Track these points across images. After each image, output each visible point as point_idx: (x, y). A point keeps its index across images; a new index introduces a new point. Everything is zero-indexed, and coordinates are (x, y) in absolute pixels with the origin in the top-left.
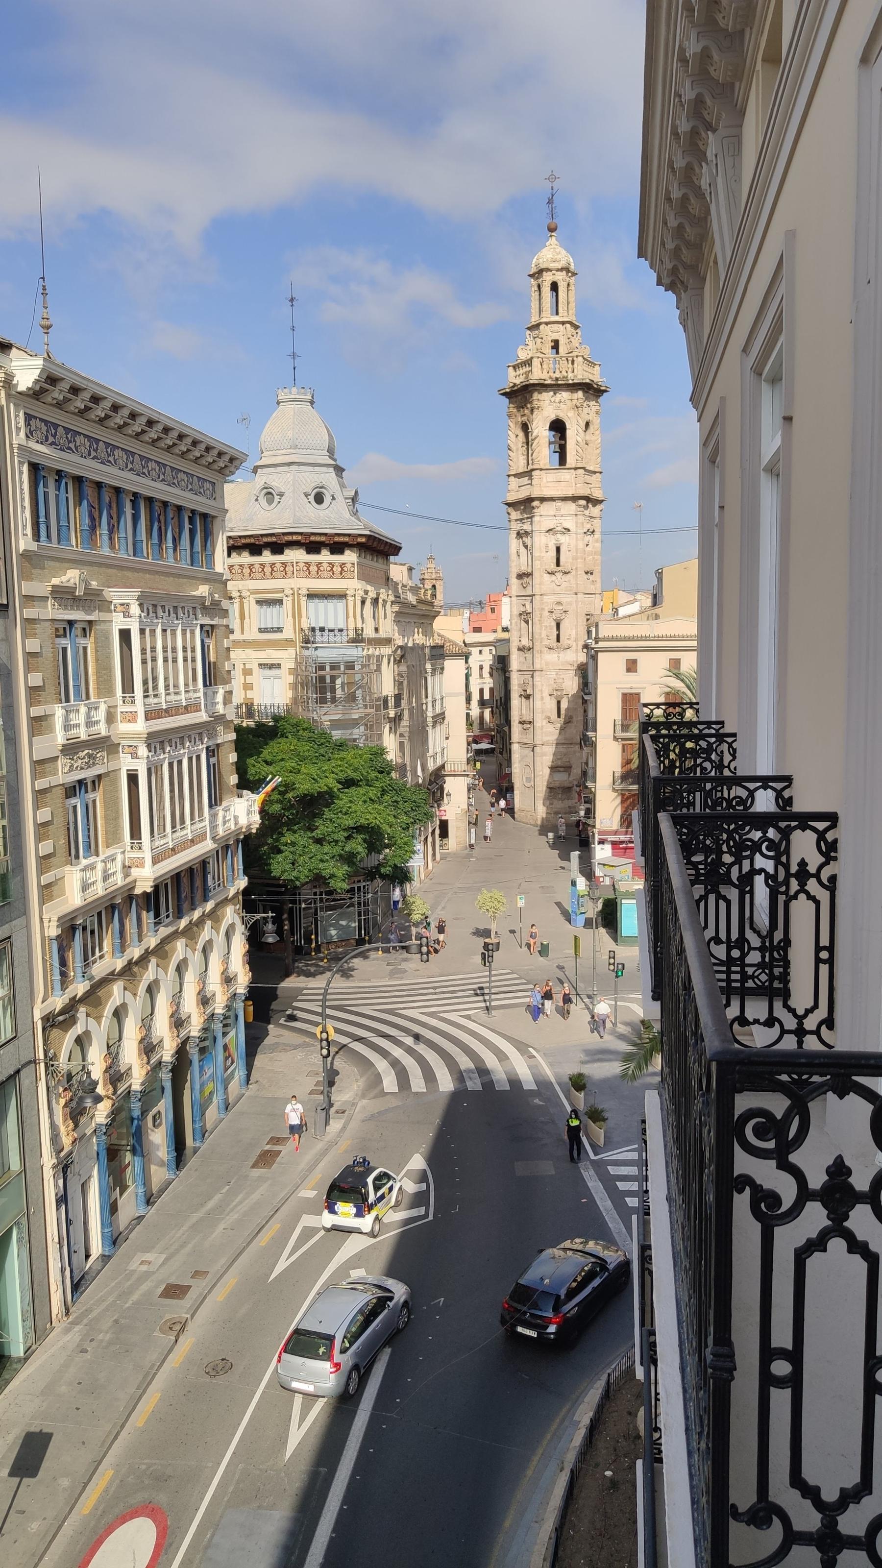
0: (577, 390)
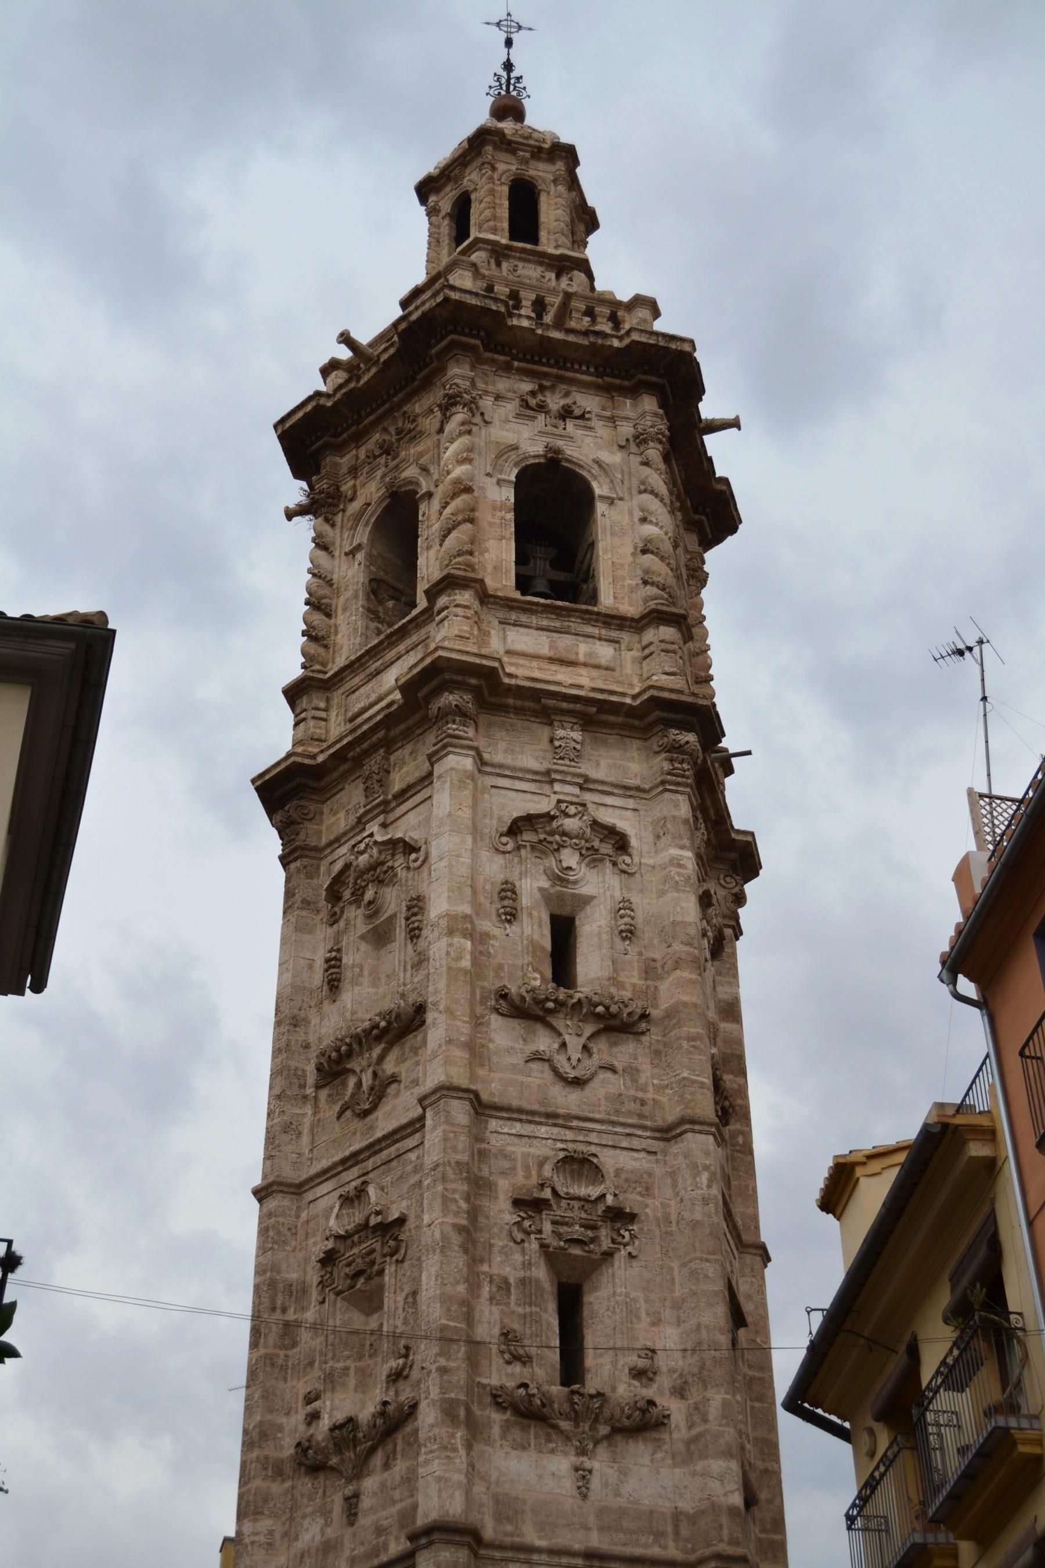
0: (633, 392)
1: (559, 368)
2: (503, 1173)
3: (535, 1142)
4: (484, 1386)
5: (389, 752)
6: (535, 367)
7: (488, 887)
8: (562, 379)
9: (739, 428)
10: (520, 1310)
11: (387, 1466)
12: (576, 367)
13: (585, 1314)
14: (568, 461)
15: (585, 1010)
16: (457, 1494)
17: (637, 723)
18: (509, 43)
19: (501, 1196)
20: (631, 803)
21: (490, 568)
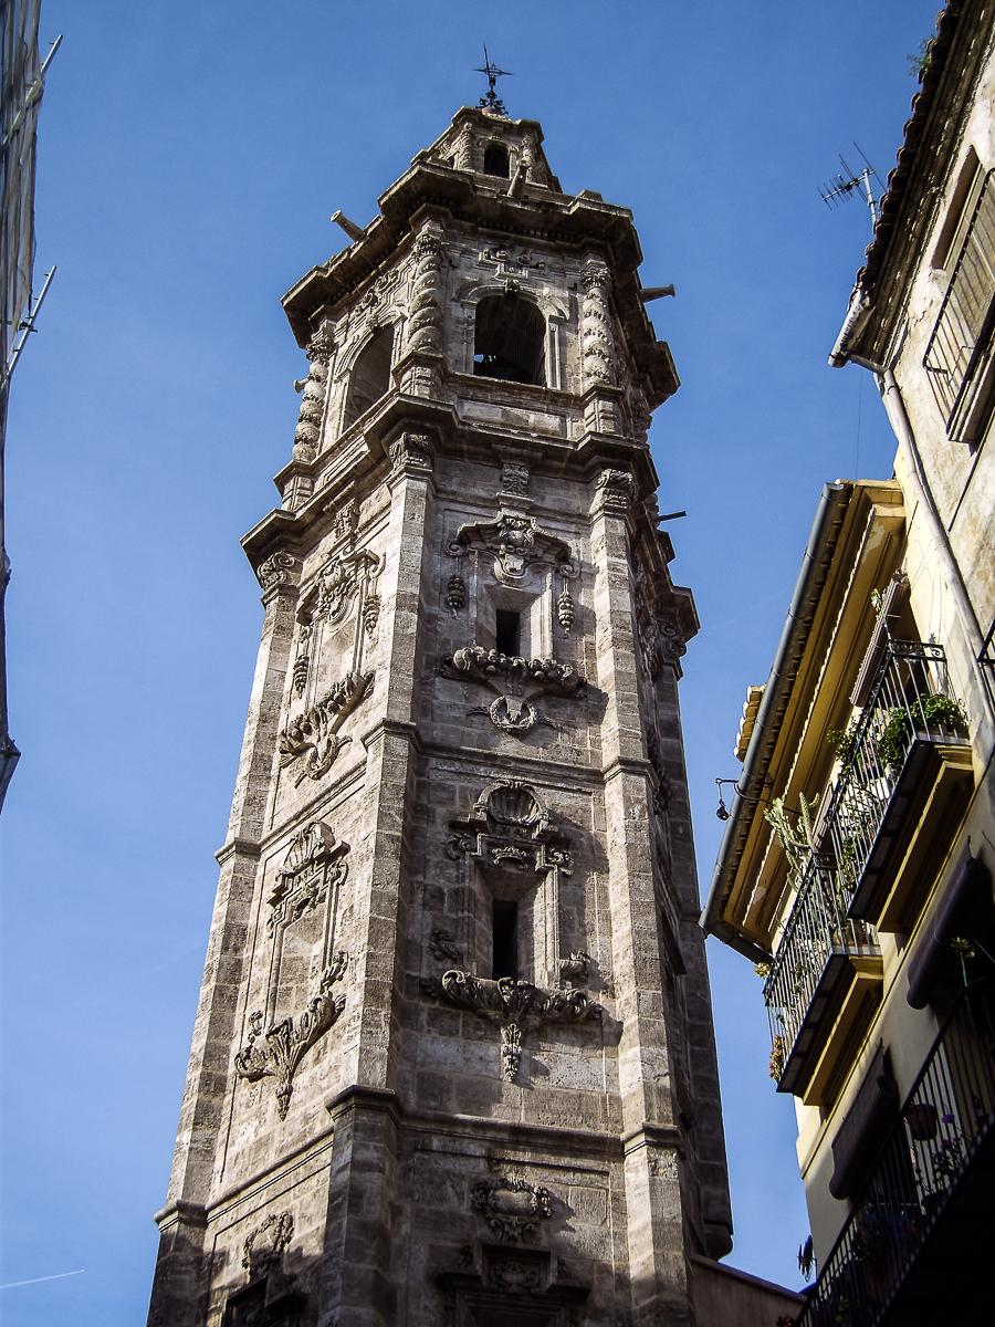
0: (580, 253)
1: (518, 233)
2: (442, 803)
3: (474, 779)
4: (413, 978)
5: (359, 502)
7: (438, 581)
8: (521, 243)
9: (673, 294)
10: (453, 916)
12: (532, 232)
14: (523, 295)
15: (525, 674)
16: (378, 1065)
17: (579, 468)
18: (493, 81)
19: (438, 821)
20: (573, 528)
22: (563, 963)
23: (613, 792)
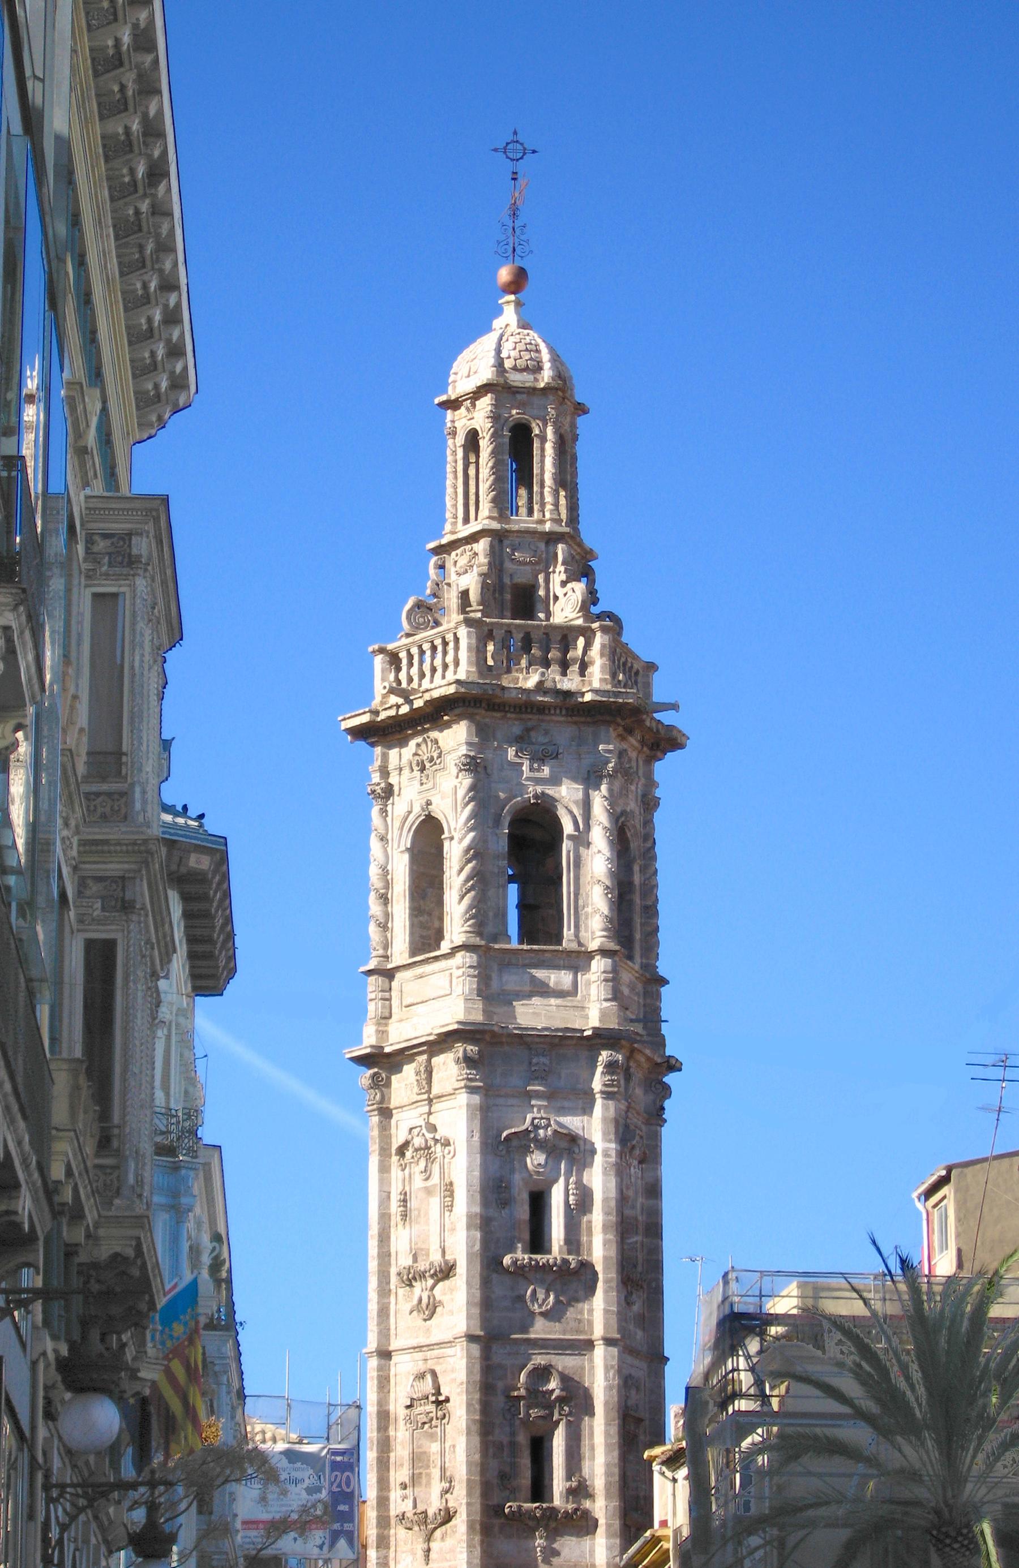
6: (524, 716)
8: (543, 721)
11: (443, 1539)
13: (545, 1454)
21: (491, 914)
22: (568, 1484)
23: (600, 1351)
